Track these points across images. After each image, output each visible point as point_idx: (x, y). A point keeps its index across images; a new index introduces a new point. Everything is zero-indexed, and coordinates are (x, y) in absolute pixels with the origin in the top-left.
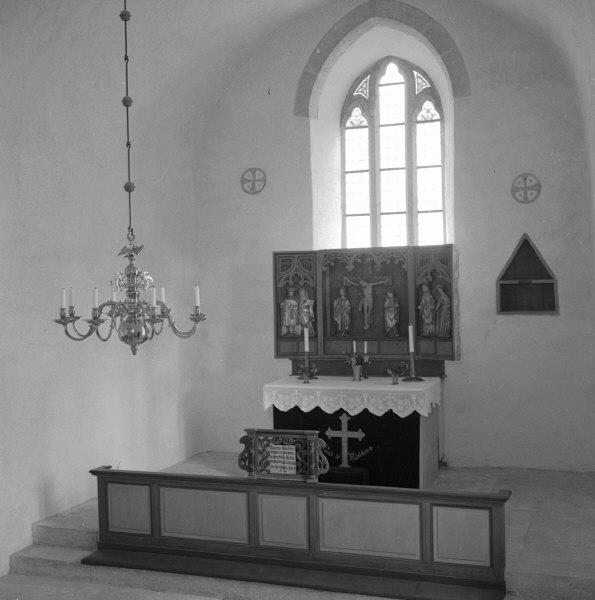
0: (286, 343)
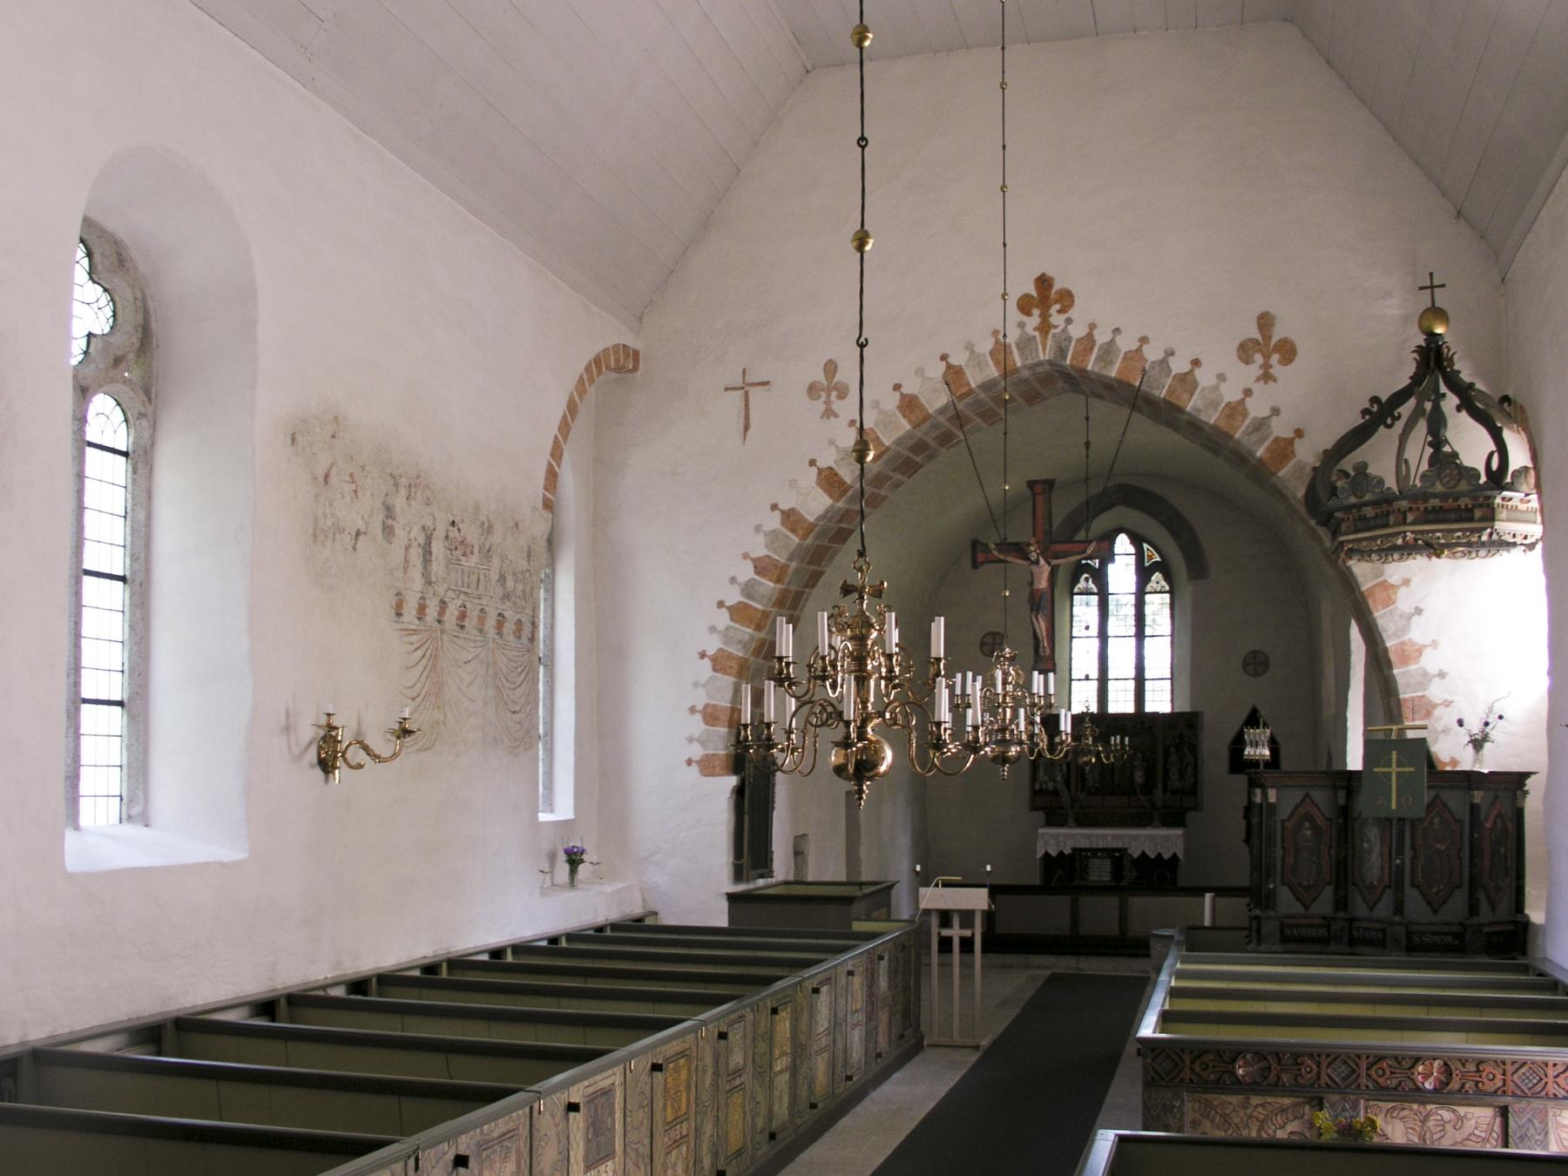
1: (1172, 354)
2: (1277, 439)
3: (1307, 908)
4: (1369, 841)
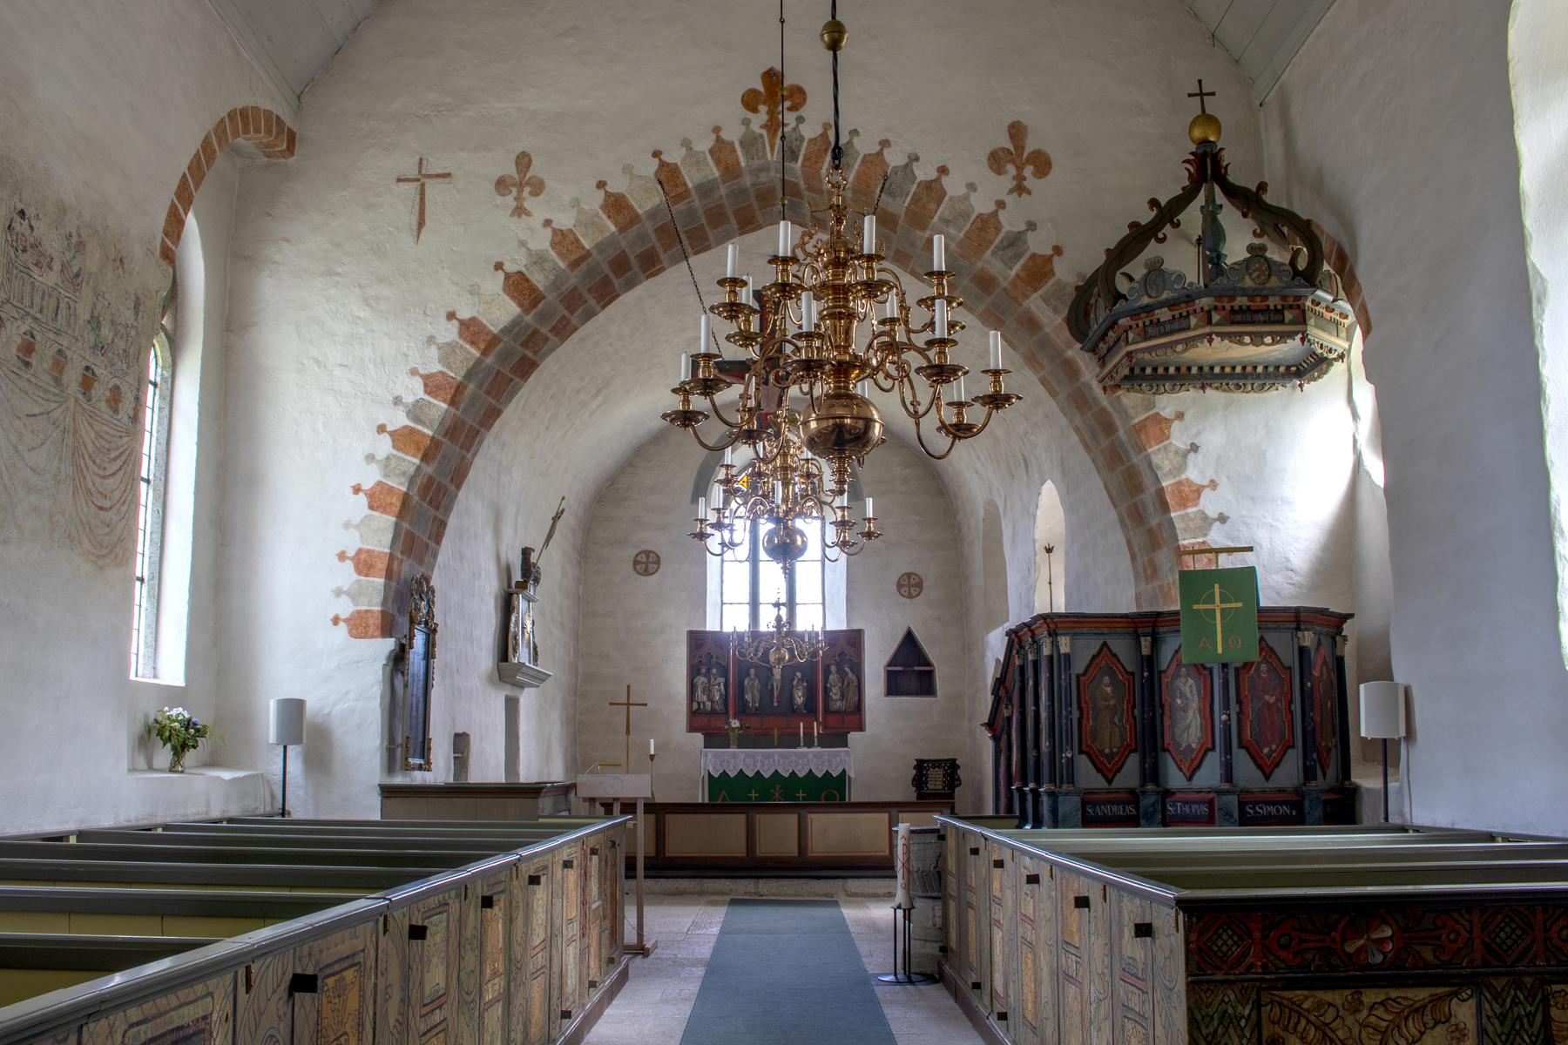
0: (699, 719)
1: (917, 159)
2: (1034, 256)
3: (1110, 781)
4: (1182, 695)
